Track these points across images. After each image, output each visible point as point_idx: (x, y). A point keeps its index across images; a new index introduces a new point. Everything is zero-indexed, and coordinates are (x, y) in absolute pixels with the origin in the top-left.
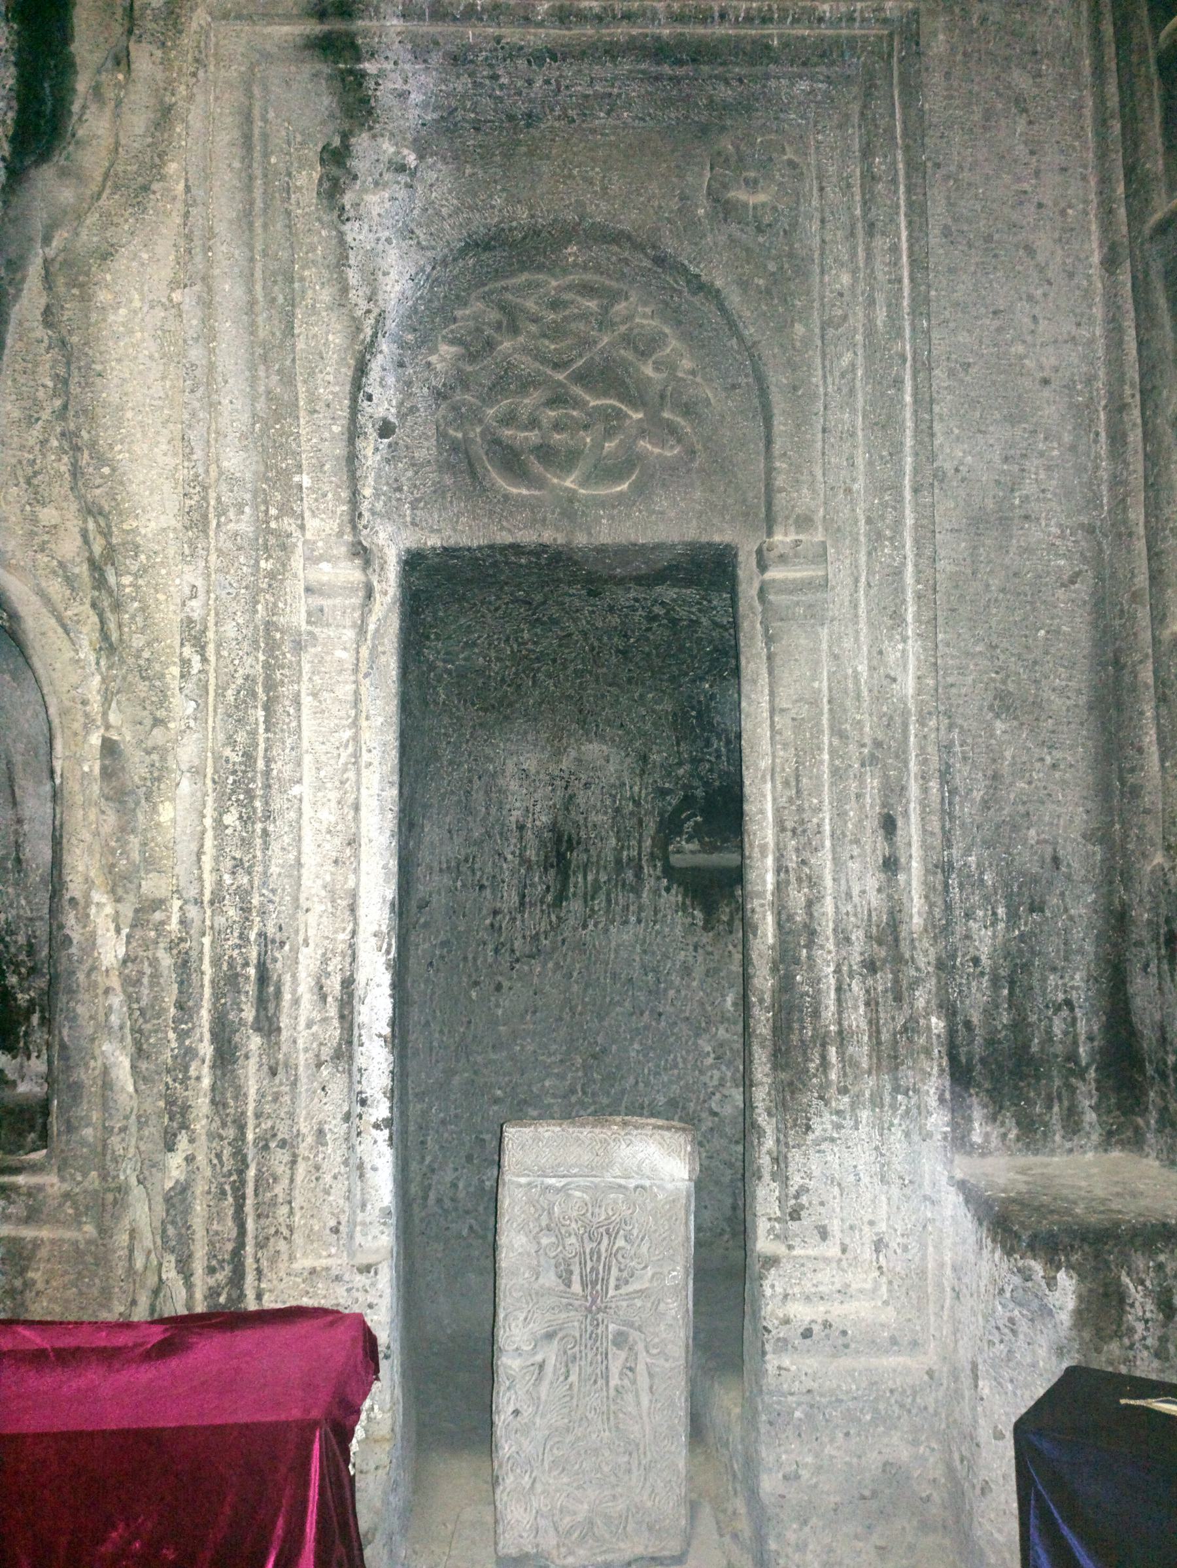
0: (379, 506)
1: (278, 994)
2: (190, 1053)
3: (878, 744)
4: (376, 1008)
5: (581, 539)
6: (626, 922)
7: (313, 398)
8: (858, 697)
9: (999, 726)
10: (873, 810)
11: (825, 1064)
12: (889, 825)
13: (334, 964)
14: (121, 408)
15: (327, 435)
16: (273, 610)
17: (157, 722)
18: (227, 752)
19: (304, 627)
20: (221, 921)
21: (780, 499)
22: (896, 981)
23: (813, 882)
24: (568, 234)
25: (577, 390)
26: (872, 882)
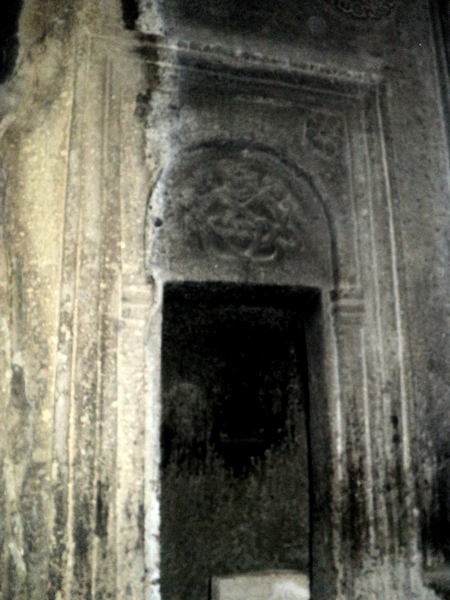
0: (154, 259)
1: (107, 515)
2: (63, 547)
3: (389, 383)
4: (153, 519)
5: (251, 280)
6: (197, 474)
7: (128, 206)
8: (379, 361)
9: (431, 376)
10: (388, 413)
11: (368, 536)
12: (395, 420)
13: (135, 498)
14: (32, 204)
15: (133, 223)
16: (106, 309)
17: (43, 366)
18: (84, 383)
19: (120, 318)
20: (79, 475)
21: (342, 270)
22: (400, 493)
23: (362, 449)
24: (244, 145)
25: (250, 213)
26: (388, 447)
